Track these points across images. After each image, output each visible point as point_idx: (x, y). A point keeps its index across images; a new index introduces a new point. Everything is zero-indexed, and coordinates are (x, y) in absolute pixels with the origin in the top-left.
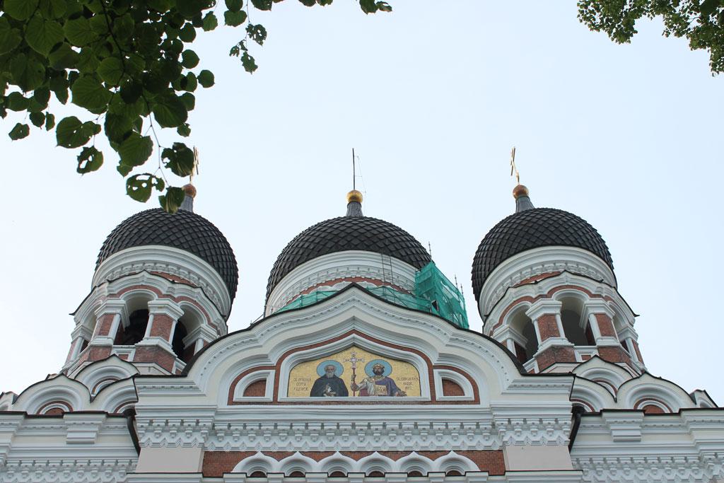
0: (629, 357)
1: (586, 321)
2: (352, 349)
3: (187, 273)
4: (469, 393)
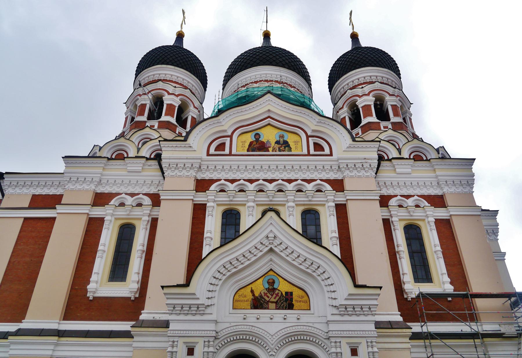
0: (407, 127)
3: (182, 80)
4: (327, 151)
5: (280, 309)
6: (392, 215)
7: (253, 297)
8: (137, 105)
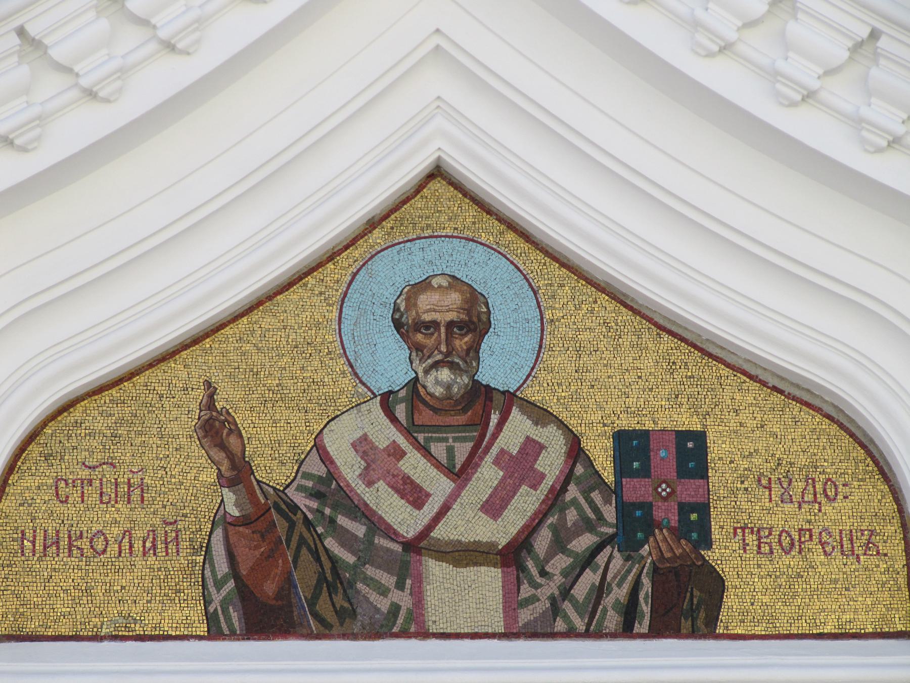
5: (560, 625)
7: (229, 497)
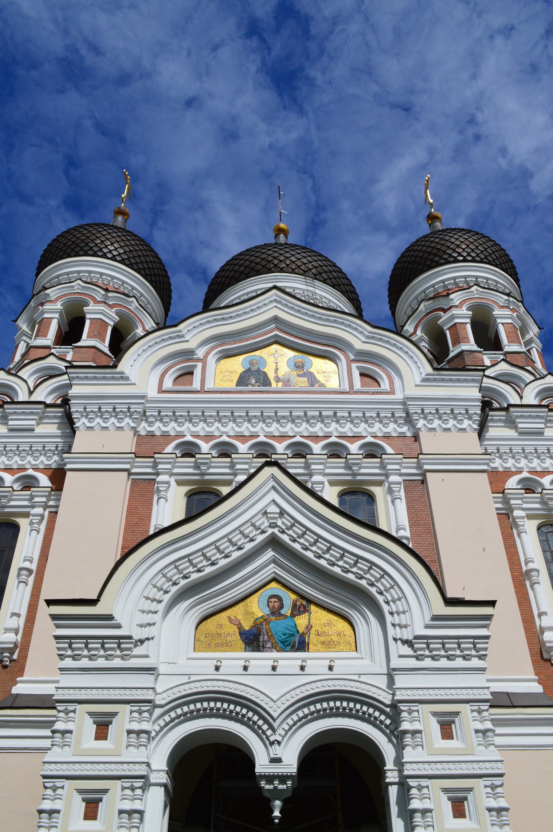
0: (534, 362)
1: (495, 331)
2: (274, 345)
4: (385, 385)
6: (512, 506)
8: (36, 321)
